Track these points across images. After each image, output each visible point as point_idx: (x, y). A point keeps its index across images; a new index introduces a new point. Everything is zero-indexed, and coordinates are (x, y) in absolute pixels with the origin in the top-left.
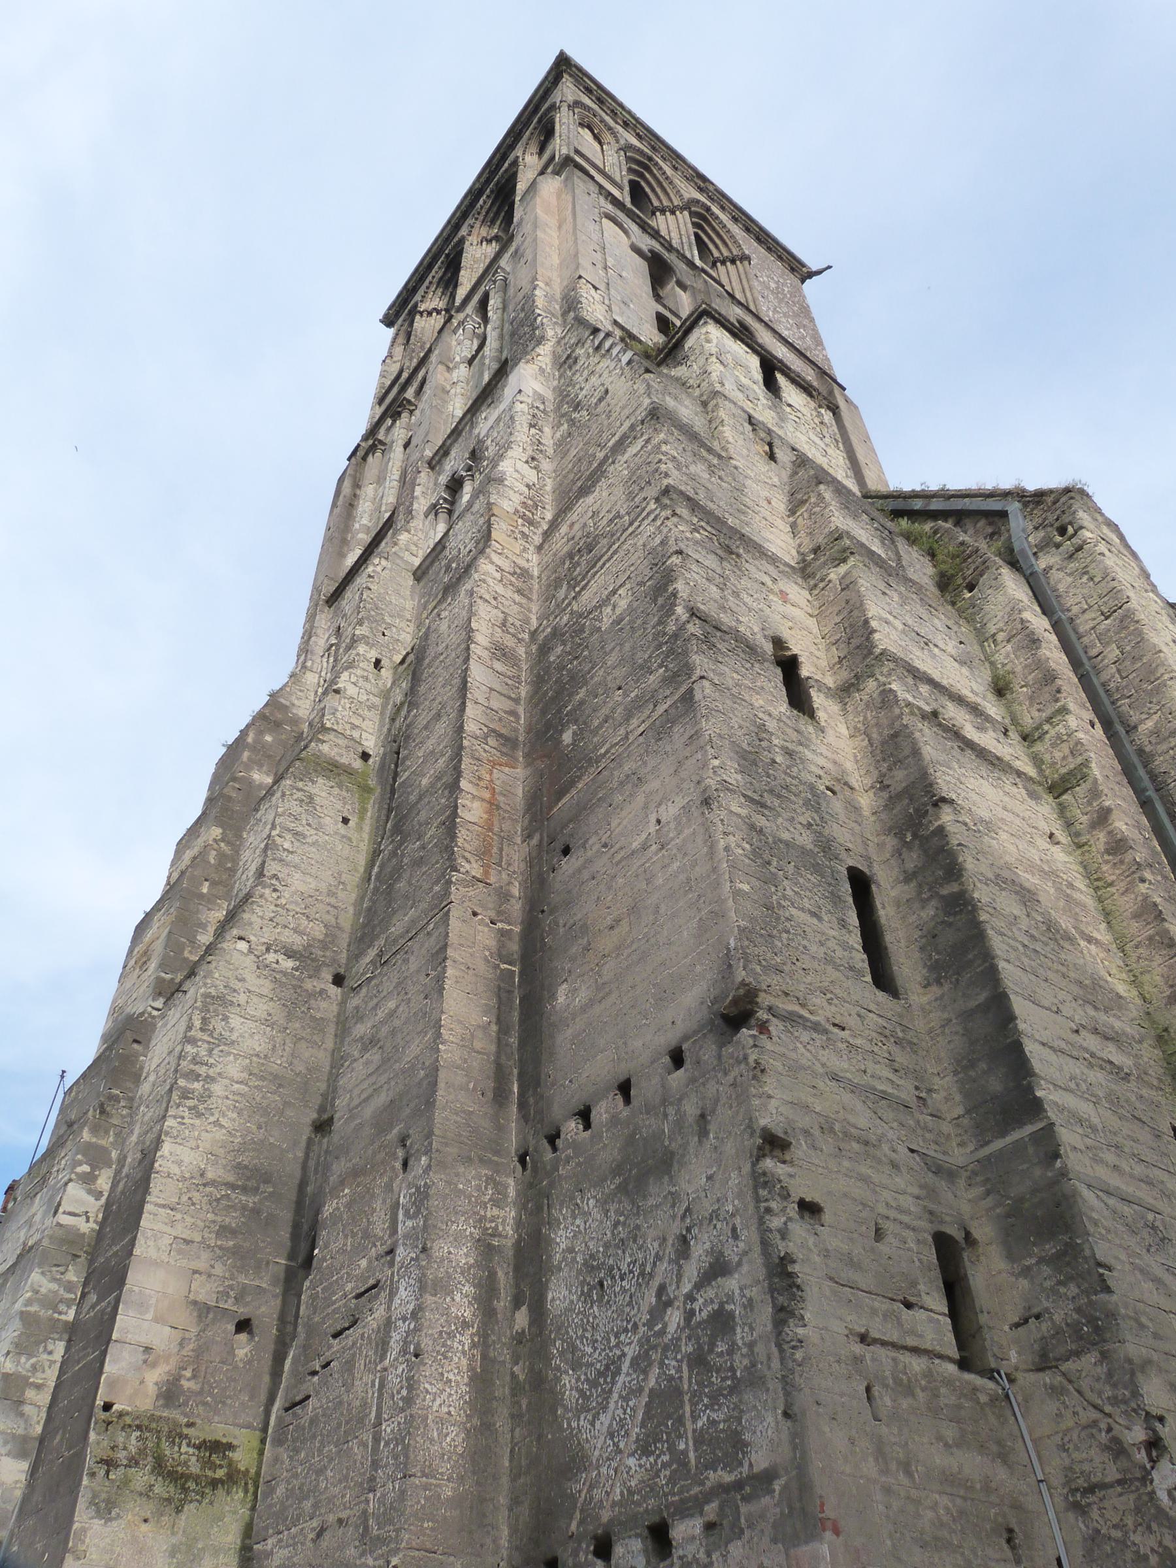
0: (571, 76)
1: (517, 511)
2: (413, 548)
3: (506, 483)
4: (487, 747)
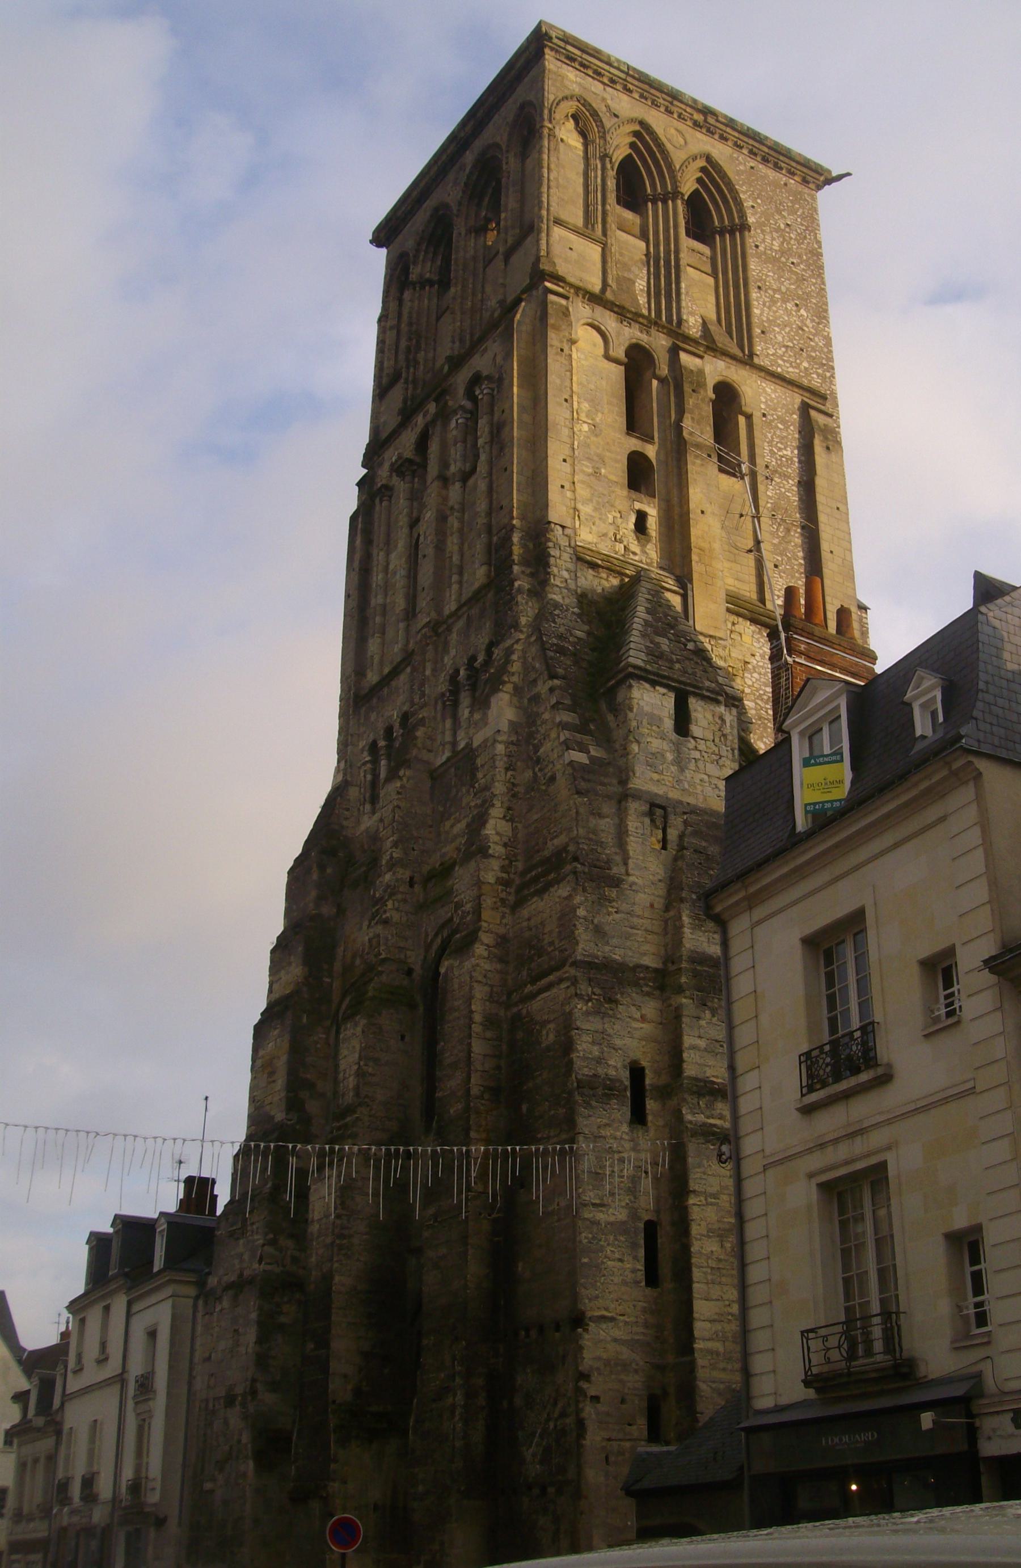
0: (552, 49)
2: (429, 742)
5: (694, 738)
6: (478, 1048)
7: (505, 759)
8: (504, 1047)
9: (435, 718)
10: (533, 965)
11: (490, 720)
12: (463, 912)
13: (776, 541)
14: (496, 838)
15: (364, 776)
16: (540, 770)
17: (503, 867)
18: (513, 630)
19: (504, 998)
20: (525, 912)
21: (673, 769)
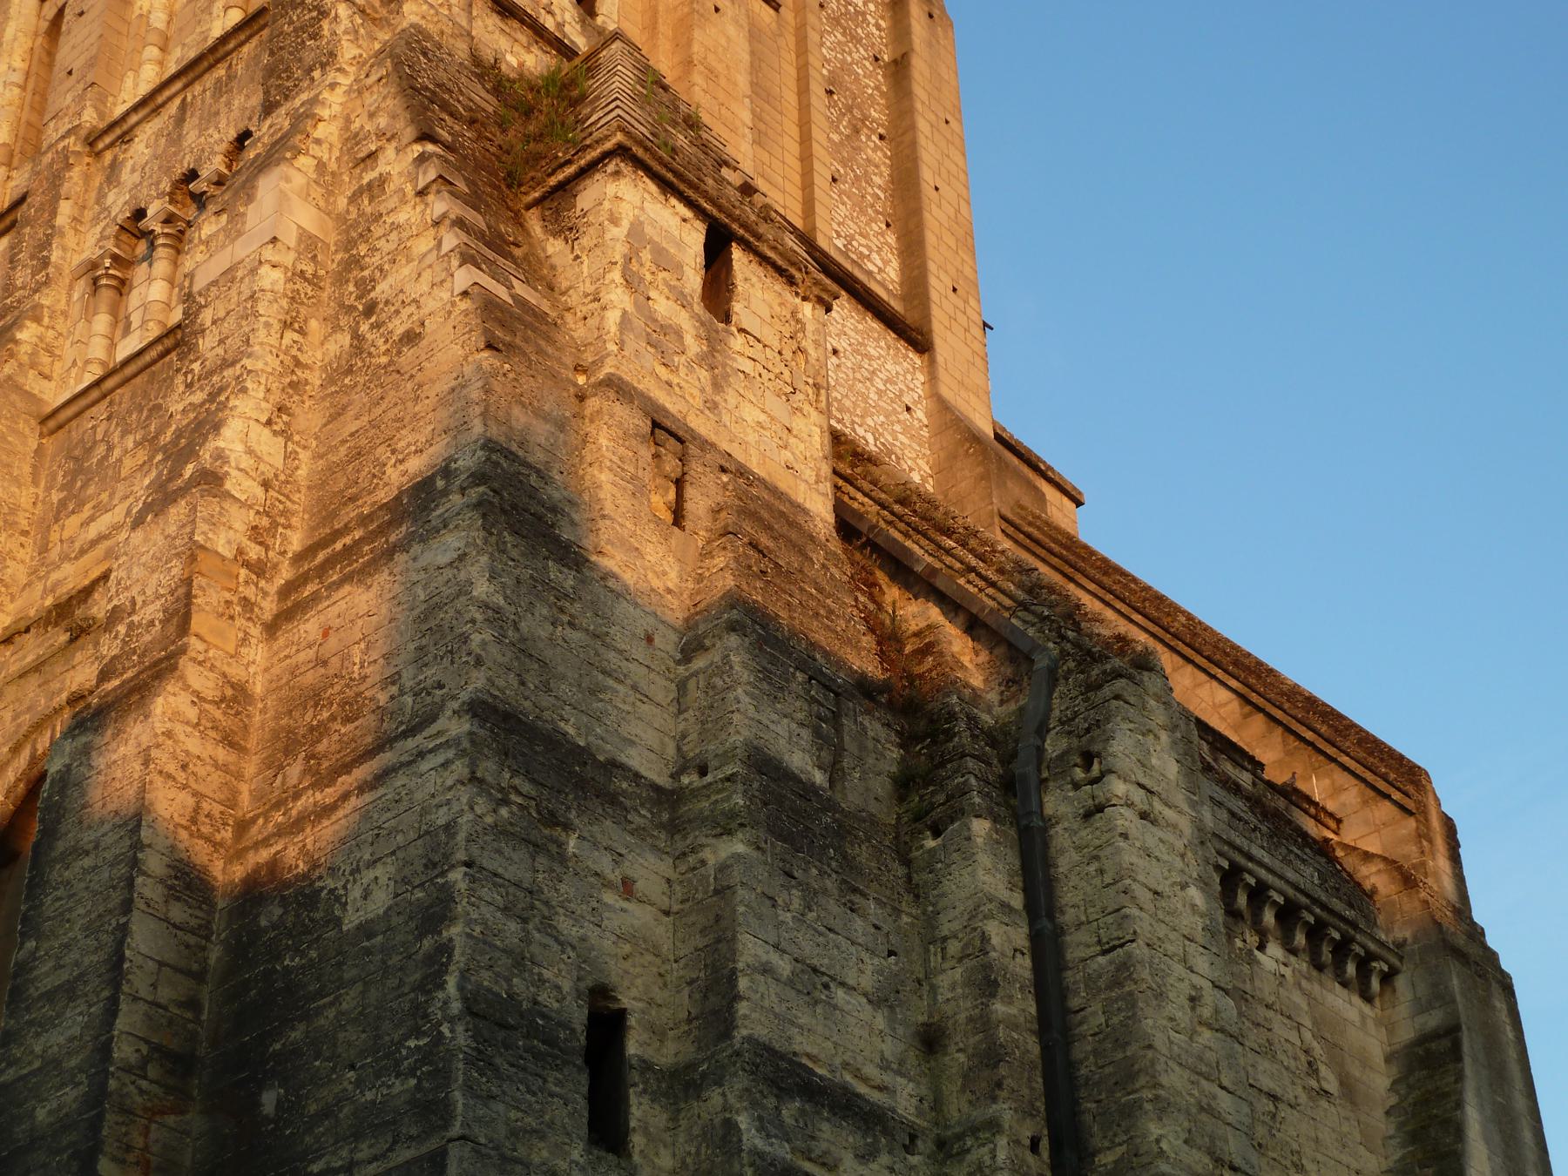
1: (240, 551)
2: (45, 359)
3: (228, 485)
4: (144, 1084)
5: (742, 330)
6: (144, 939)
7: (284, 303)
8: (215, 954)
10: (321, 747)
11: (248, 226)
12: (131, 626)
13: (835, 137)
14: (247, 462)
17: (255, 528)
18: (316, 74)
19: (227, 834)
20: (309, 627)
21: (704, 374)
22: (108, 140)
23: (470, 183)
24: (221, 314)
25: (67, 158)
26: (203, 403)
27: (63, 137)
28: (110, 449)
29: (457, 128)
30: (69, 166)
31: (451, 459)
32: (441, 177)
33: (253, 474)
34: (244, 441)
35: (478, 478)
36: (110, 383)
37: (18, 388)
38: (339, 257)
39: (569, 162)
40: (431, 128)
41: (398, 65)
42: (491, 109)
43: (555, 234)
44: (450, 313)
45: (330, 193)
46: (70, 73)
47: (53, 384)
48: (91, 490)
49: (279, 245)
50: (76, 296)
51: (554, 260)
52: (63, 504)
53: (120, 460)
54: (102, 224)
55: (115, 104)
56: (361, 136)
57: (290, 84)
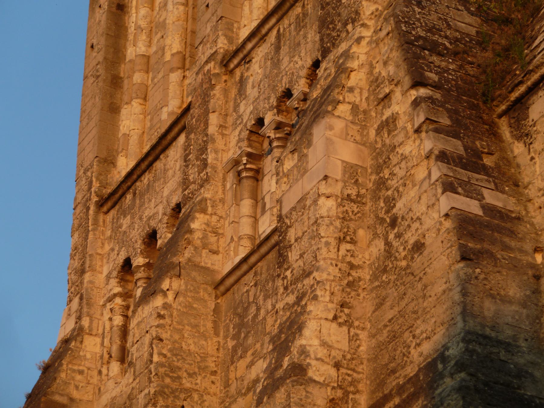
2: (213, 239)
3: (310, 373)
7: (338, 223)
9: (222, 201)
11: (310, 165)
14: (322, 353)
15: (108, 319)
16: (399, 236)
17: (332, 400)
18: (350, 27)
22: (236, 61)
23: (453, 114)
24: (300, 234)
25: (210, 80)
26: (294, 305)
27: (207, 62)
28: (258, 309)
29: (443, 64)
30: (212, 87)
31: (446, 348)
32: (427, 119)
33: (327, 360)
34: (320, 337)
35: (460, 366)
36: (253, 259)
37: (197, 267)
38: (373, 177)
39: (521, 83)
40: (422, 75)
41: (398, 23)
42: (473, 31)
43: (519, 138)
44: (439, 230)
45: (364, 127)
46: (207, 6)
47: (221, 255)
48: (250, 341)
49: (329, 180)
50: (228, 186)
51: (520, 160)
52: (235, 349)
53: (264, 319)
54: (239, 129)
55: (239, 28)
56: (379, 81)
57: (334, 34)
